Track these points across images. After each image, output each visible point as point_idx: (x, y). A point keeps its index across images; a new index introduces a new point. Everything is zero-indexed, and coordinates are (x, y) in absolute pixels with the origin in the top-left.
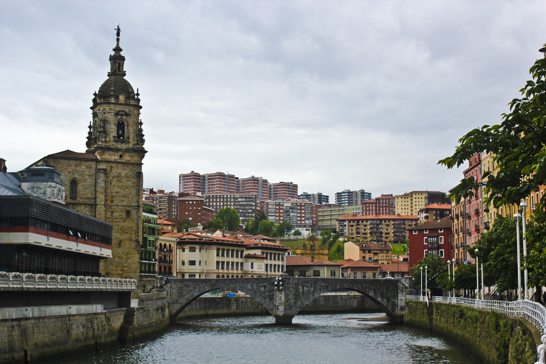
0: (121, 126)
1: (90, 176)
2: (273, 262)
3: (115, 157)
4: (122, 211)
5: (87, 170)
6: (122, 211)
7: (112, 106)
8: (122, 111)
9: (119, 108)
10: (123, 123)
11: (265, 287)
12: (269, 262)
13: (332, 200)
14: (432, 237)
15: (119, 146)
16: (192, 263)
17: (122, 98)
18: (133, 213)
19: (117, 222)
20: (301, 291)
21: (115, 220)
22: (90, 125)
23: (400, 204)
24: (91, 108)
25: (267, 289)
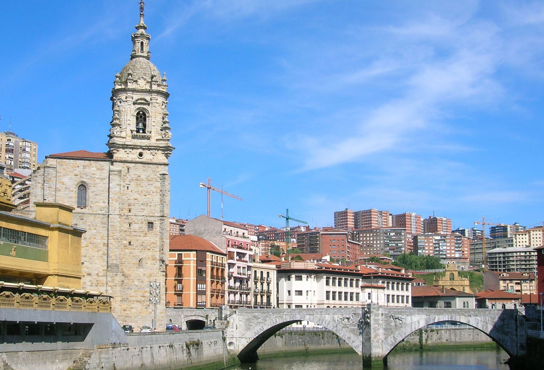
1: (102, 179)
2: (396, 293)
3: (133, 155)
4: (142, 223)
5: (99, 172)
6: (142, 223)
7: (130, 94)
8: (141, 99)
9: (136, 96)
16: (300, 293)
18: (157, 224)
19: (137, 236)
21: (133, 233)
25: (351, 322)
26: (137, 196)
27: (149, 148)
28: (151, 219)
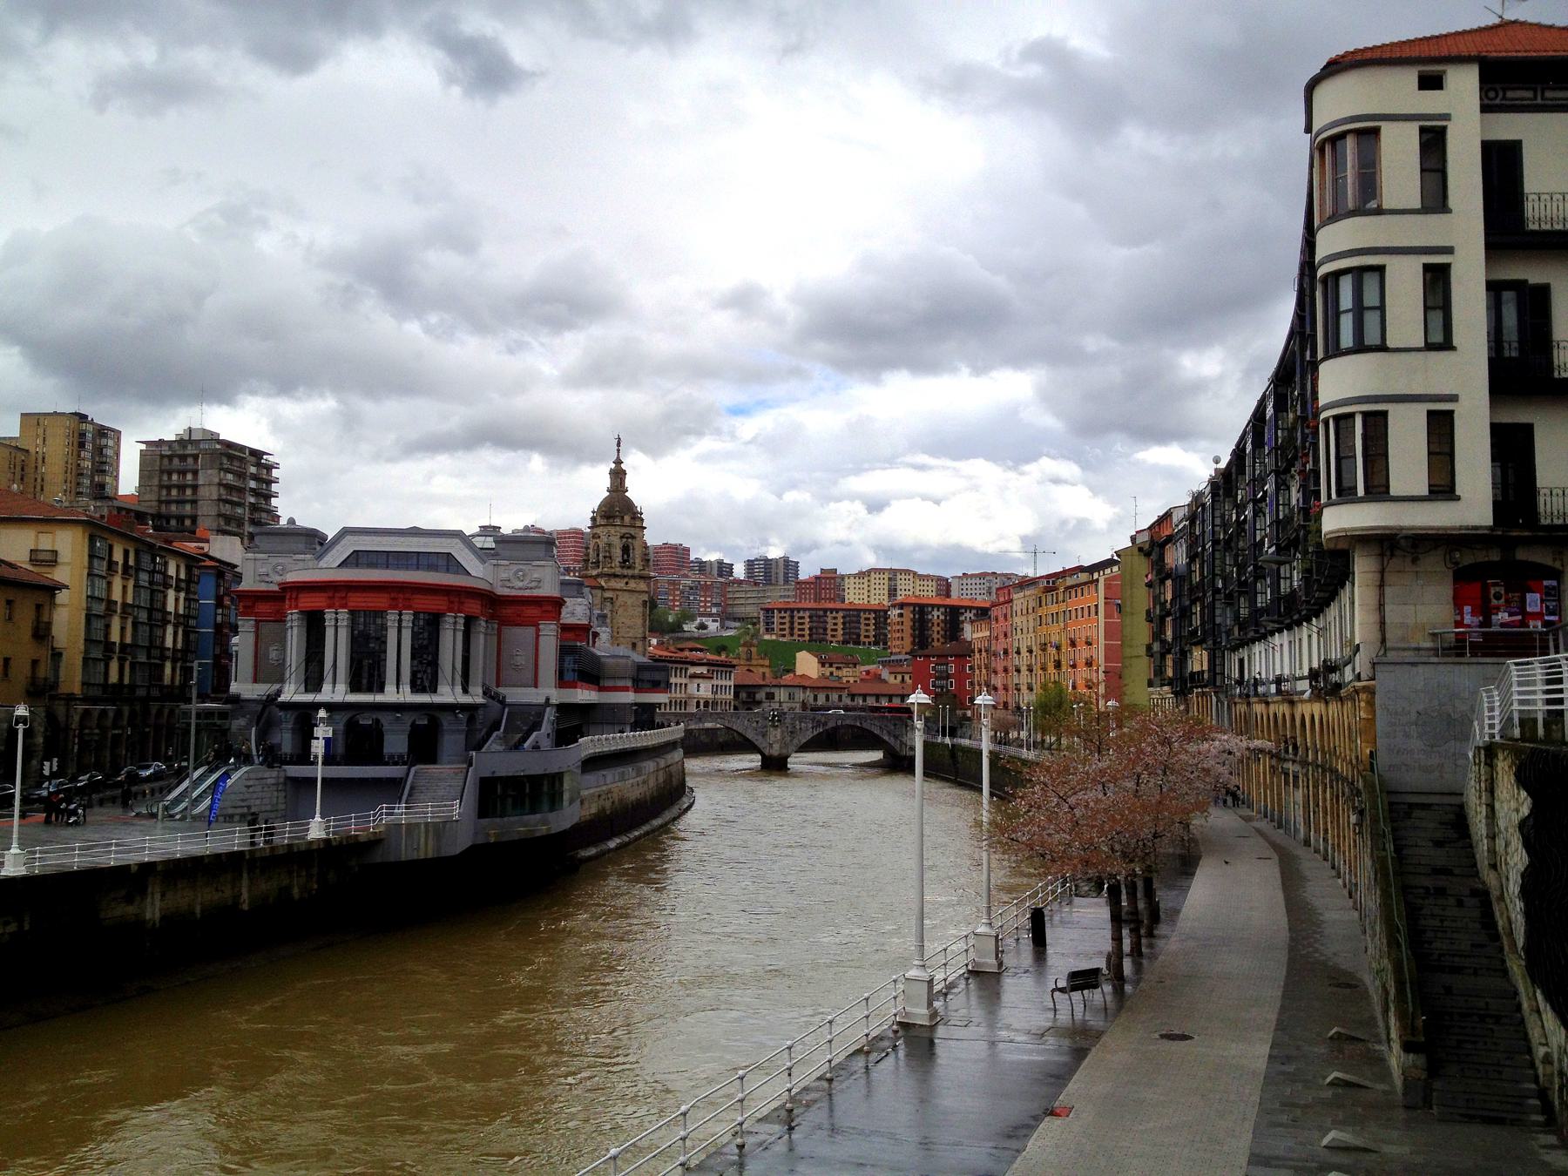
0: (626, 550)
3: (620, 584)
9: (624, 530)
10: (628, 546)
11: (757, 722)
12: (715, 682)
13: (739, 571)
14: (942, 665)
15: (625, 572)
17: (627, 518)
20: (798, 727)
23: (852, 586)
26: (624, 620)
27: (633, 577)
28: (634, 640)
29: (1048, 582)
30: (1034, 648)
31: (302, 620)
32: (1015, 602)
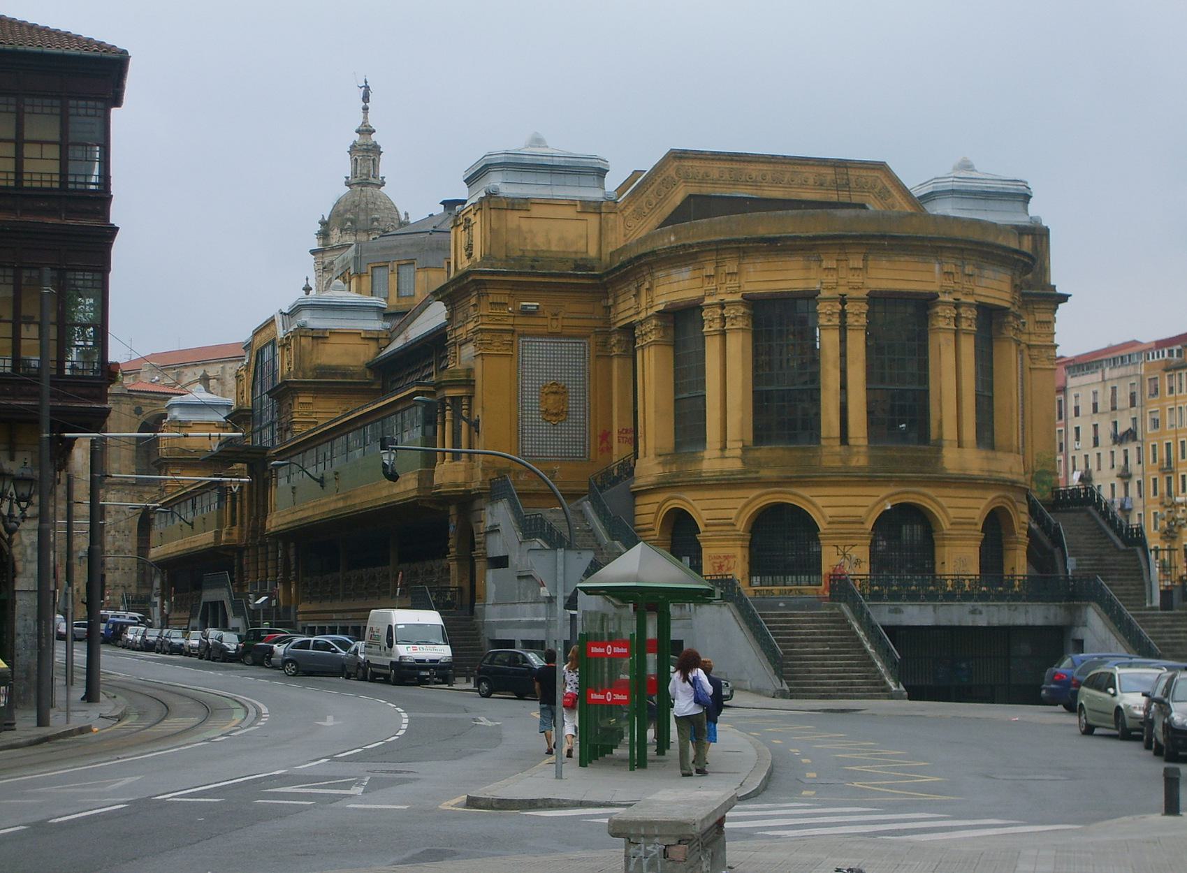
22: (307, 285)
24: (313, 252)
29: (1171, 353)
30: (1134, 466)
31: (665, 328)
32: (1071, 394)
